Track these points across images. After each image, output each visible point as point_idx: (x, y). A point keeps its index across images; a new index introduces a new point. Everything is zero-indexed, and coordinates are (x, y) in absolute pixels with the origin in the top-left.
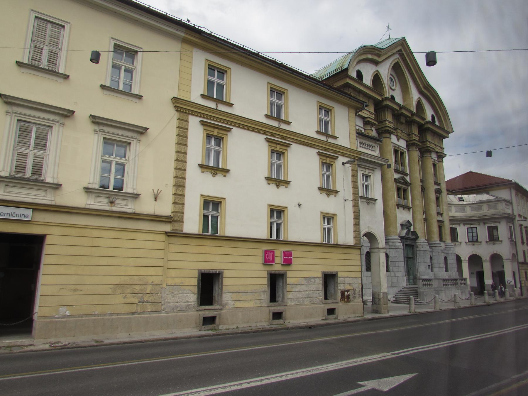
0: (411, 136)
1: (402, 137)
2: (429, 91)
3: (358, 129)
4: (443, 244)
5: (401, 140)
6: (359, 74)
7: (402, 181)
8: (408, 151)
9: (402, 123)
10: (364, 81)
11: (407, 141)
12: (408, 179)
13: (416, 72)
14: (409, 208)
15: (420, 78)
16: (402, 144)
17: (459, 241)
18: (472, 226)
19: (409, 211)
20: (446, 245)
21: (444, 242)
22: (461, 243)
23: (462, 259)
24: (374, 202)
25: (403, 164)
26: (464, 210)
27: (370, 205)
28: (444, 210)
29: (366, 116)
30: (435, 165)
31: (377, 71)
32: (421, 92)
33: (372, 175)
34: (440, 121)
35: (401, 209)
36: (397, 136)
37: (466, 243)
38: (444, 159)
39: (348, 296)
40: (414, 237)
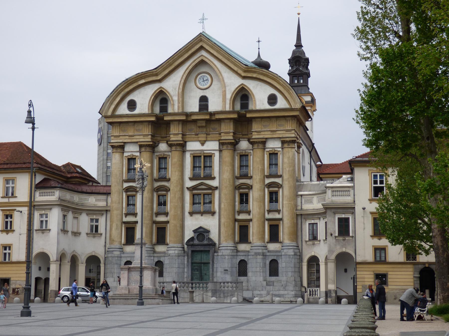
2: (255, 72)
4: (273, 246)
5: (207, 143)
9: (202, 127)
11: (219, 140)
13: (228, 60)
14: (213, 213)
15: (235, 65)
16: (212, 146)
17: (318, 239)
20: (282, 246)
21: (281, 242)
22: (320, 241)
27: (45, 234)
28: (284, 206)
31: (161, 87)
33: (48, 213)
35: (198, 216)
36: (200, 141)
37: (324, 240)
39: (18, 291)
40: (210, 243)
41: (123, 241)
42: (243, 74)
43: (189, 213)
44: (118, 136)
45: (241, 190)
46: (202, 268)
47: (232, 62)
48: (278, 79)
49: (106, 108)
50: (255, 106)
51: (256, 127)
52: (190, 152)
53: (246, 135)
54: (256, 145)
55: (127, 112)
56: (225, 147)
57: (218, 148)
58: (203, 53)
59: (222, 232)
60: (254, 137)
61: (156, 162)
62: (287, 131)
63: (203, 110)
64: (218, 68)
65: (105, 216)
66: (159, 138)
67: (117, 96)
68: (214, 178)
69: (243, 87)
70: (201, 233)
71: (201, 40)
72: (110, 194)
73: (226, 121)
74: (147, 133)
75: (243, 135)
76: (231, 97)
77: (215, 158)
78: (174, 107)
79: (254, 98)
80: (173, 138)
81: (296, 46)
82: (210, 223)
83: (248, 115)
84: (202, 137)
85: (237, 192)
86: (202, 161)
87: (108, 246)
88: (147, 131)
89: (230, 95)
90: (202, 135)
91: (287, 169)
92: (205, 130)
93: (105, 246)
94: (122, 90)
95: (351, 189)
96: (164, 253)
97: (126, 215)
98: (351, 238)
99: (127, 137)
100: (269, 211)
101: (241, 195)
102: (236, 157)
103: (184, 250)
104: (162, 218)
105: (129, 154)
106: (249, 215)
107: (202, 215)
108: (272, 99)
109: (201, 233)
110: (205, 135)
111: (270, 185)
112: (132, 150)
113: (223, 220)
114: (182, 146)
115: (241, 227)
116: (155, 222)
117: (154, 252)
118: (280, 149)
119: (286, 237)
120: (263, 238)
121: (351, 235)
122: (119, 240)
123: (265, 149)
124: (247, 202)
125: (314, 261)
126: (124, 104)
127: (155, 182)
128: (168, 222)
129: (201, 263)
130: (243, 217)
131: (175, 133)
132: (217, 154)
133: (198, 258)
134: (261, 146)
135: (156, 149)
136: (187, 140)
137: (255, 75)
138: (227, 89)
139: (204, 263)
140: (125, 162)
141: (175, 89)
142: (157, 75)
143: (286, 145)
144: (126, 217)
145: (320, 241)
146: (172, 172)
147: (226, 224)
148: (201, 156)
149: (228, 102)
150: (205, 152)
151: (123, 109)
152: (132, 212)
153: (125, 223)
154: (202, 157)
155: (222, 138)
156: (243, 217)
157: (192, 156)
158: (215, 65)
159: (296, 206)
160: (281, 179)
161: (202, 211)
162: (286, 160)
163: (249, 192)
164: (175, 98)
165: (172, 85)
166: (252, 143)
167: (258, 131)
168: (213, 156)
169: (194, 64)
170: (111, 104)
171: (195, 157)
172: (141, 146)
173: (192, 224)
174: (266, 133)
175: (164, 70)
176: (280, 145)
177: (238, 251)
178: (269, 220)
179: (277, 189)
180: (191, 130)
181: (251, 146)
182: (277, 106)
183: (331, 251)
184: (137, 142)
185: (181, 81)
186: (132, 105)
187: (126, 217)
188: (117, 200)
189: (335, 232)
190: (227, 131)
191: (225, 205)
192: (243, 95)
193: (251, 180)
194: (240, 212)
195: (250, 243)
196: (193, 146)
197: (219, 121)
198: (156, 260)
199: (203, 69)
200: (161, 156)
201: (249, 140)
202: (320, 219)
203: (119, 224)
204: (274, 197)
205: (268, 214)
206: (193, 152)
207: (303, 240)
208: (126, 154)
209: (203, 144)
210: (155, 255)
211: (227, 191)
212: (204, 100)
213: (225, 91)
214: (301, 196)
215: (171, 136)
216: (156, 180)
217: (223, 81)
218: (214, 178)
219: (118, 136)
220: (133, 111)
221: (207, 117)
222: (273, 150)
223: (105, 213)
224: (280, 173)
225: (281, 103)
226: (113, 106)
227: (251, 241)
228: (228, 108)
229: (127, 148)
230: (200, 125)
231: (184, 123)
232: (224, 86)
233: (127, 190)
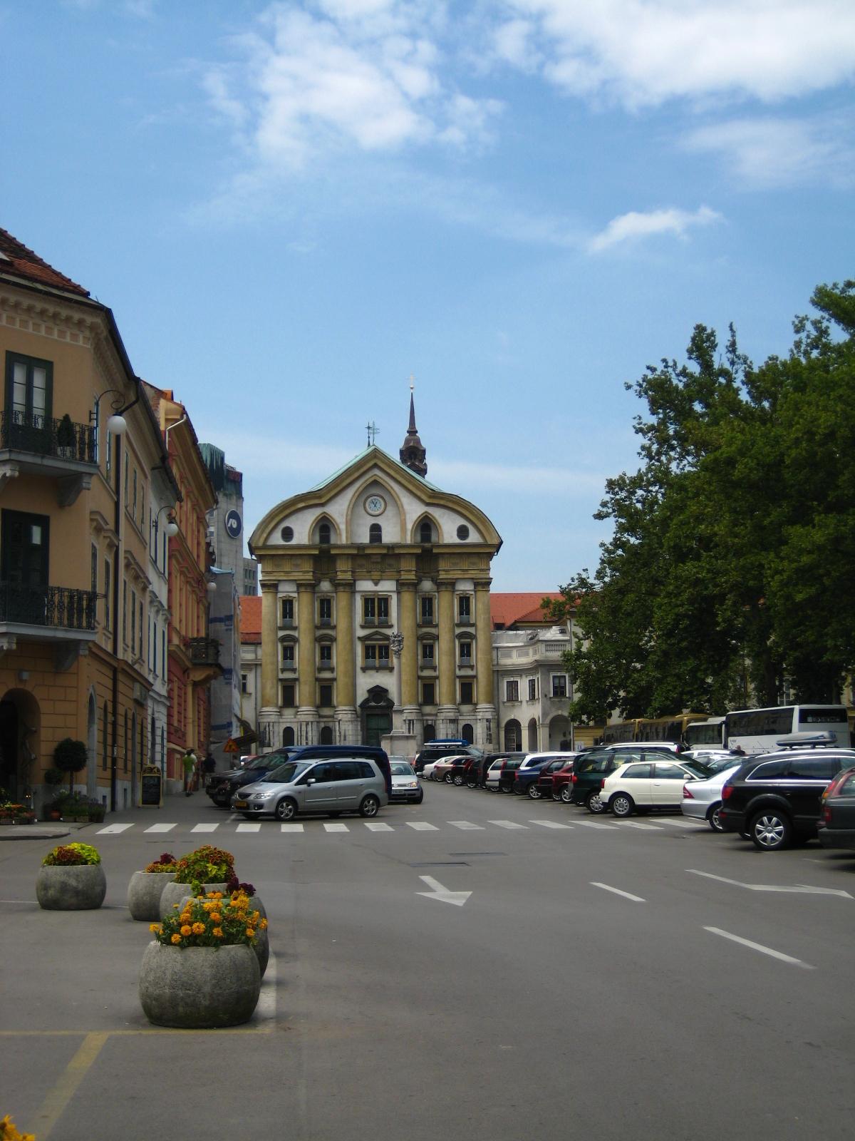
1: (384, 577)
2: (442, 499)
7: (379, 637)
9: (377, 563)
11: (397, 581)
13: (410, 482)
14: (391, 669)
22: (521, 702)
23: (522, 726)
26: (527, 654)
28: (479, 660)
36: (373, 580)
37: (527, 701)
41: (280, 703)
42: (428, 500)
43: (362, 668)
45: (425, 641)
47: (414, 485)
49: (257, 537)
50: (443, 541)
51: (443, 565)
52: (361, 594)
53: (428, 573)
54: (444, 587)
55: (282, 542)
56: (405, 589)
57: (395, 589)
58: (377, 472)
59: (403, 691)
60: (441, 577)
61: (317, 605)
62: (482, 570)
63: (375, 542)
64: (395, 491)
65: (254, 671)
66: (319, 575)
68: (391, 626)
69: (426, 516)
70: (378, 693)
71: (375, 457)
72: (260, 644)
73: (407, 556)
75: (425, 573)
76: (413, 528)
77: (393, 600)
78: (341, 538)
79: (441, 530)
80: (340, 576)
81: (408, 432)
82: (388, 681)
83: (435, 551)
84: (376, 575)
85: (419, 643)
86: (376, 607)
87: (258, 708)
88: (308, 566)
89: (412, 524)
90: (376, 573)
91: (482, 617)
92: (379, 566)
93: (256, 708)
94: (277, 515)
95: (567, 643)
96: (332, 717)
97: (283, 670)
98: (567, 700)
99: (282, 574)
100: (461, 667)
101: (425, 647)
102: (418, 601)
103: (356, 714)
104: (327, 675)
105: (284, 594)
106: (435, 671)
108: (463, 532)
109: (378, 693)
110: (379, 573)
111: (461, 636)
112: (287, 590)
113: (404, 678)
114: (351, 587)
115: (425, 686)
116: (317, 679)
117: (320, 716)
118: (473, 593)
119: (482, 697)
120: (454, 698)
121: (567, 696)
122: (275, 702)
123: (454, 592)
124: (432, 655)
125: (514, 725)
127: (316, 630)
128: (334, 679)
129: (378, 729)
130: (427, 673)
131: (343, 571)
132: (394, 597)
133: (374, 723)
134: (450, 588)
135: (317, 589)
136: (357, 578)
137: (442, 502)
138: (408, 516)
139: (381, 730)
140: (280, 605)
141: (342, 515)
142: (320, 497)
143: (480, 588)
144: (282, 672)
145: (521, 702)
146: (339, 616)
148: (374, 599)
149: (409, 533)
150: (380, 593)
151: (277, 539)
153: (281, 680)
154: (376, 600)
155: (402, 577)
156: (427, 673)
157: (363, 598)
158: (392, 488)
159: (492, 660)
160: (474, 628)
161: (377, 665)
162: (480, 606)
163: (434, 643)
164: (343, 527)
165: (338, 510)
166: (439, 584)
167: (446, 570)
169: (365, 485)
170: (262, 533)
171: (368, 601)
172: (299, 586)
173: (366, 682)
174: (456, 572)
175: (329, 492)
176: (472, 587)
177: (423, 715)
178: (460, 677)
179: (469, 640)
180: (361, 566)
181: (435, 588)
182: (468, 541)
183: (545, 714)
184: (296, 580)
185: (349, 505)
186: (288, 534)
187: (282, 672)
188: (269, 652)
189: (549, 692)
190: (409, 570)
192: (426, 526)
193: (437, 629)
194: (423, 668)
195: (436, 705)
196: (365, 586)
197: (399, 557)
198: (322, 725)
199: (375, 491)
200: (322, 598)
201: (435, 581)
202: (521, 676)
203: (275, 681)
204: (466, 650)
205: (460, 670)
207: (500, 701)
208: (280, 595)
209: (376, 584)
210: (322, 720)
211: (408, 643)
212: (376, 529)
213: (405, 519)
214: (497, 648)
215: (338, 573)
216: (317, 628)
217: (403, 507)
218: (391, 626)
220: (289, 541)
221: (385, 551)
222: (465, 593)
223: (254, 667)
224: (472, 621)
225: (474, 537)
226: (265, 535)
228: (409, 541)
229: (281, 588)
230: (375, 560)
231: (353, 557)
232: (400, 512)
233: (283, 639)
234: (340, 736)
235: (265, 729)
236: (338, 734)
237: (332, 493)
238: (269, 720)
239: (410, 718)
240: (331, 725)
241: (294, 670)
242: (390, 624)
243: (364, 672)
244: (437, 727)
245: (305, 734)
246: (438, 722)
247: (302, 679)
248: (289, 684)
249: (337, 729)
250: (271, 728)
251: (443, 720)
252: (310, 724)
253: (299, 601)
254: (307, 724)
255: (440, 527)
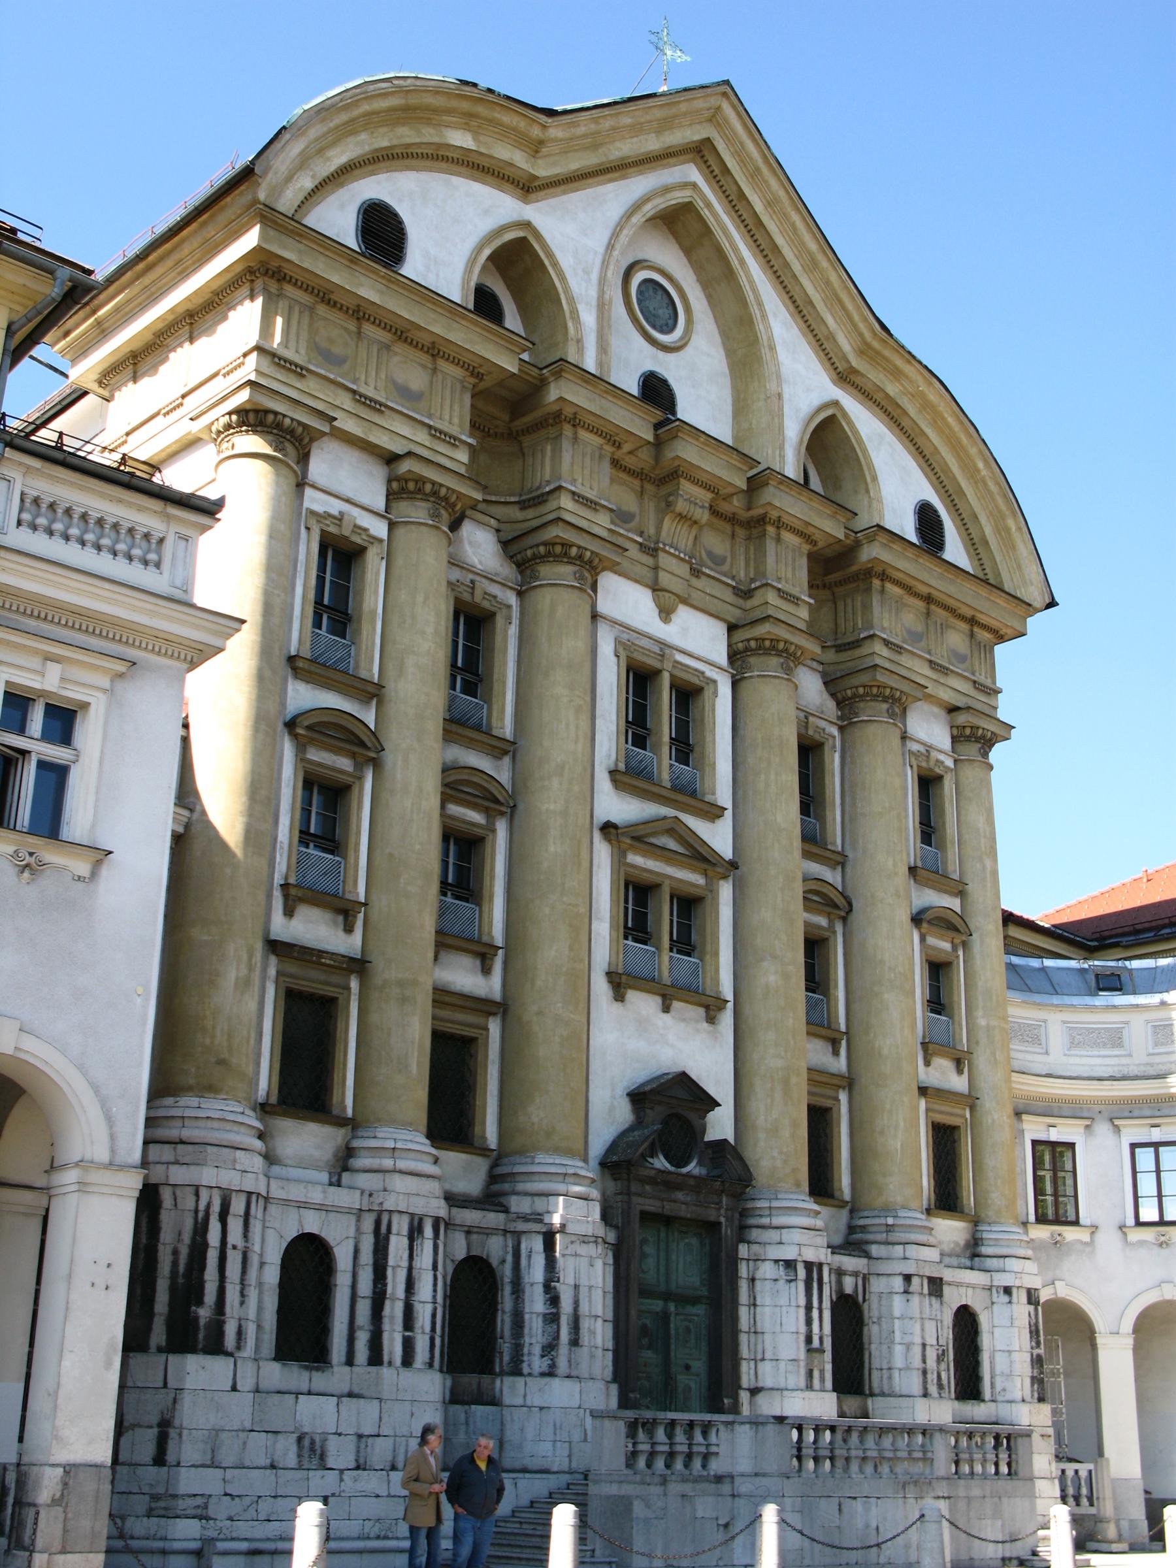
0: (755, 601)
1: (696, 596)
2: (896, 374)
3: (340, 519)
6: (382, 233)
7: (672, 844)
8: (735, 684)
10: (413, 267)
11: (732, 628)
12: (719, 837)
13: (812, 266)
16: (698, 639)
17: (1084, 1218)
18: (1156, 1135)
19: (711, 1019)
24: (82, 867)
25: (686, 747)
28: (982, 1037)
29: (398, 447)
30: (928, 784)
31: (528, 225)
32: (845, 377)
34: (974, 544)
38: (997, 753)
43: (611, 976)
44: (299, 371)
46: (672, 1325)
48: (973, 451)
54: (885, 706)
67: (349, 129)
74: (454, 430)
105: (335, 507)
107: (666, 1009)
112: (348, 484)
126: (342, 207)
144: (289, 912)
147: (794, 1080)
152: (325, 885)
158: (742, 262)
168: (708, 693)
172: (400, 489)
187: (289, 912)
191: (786, 976)
206: (625, 636)
219: (299, 371)
227: (847, 1194)
234: (552, 1318)
235: (201, 1229)
236: (536, 1303)
237: (574, 164)
238: (228, 1178)
239: (810, 1255)
240: (495, 1249)
241: (345, 912)
242: (708, 798)
243: (619, 996)
244: (872, 1309)
245: (400, 1292)
246: (877, 1285)
247: (385, 971)
248: (314, 981)
249: (536, 1273)
250: (235, 1226)
251: (908, 1278)
252: (428, 1231)
253: (389, 559)
254: (415, 1232)
255: (875, 478)
